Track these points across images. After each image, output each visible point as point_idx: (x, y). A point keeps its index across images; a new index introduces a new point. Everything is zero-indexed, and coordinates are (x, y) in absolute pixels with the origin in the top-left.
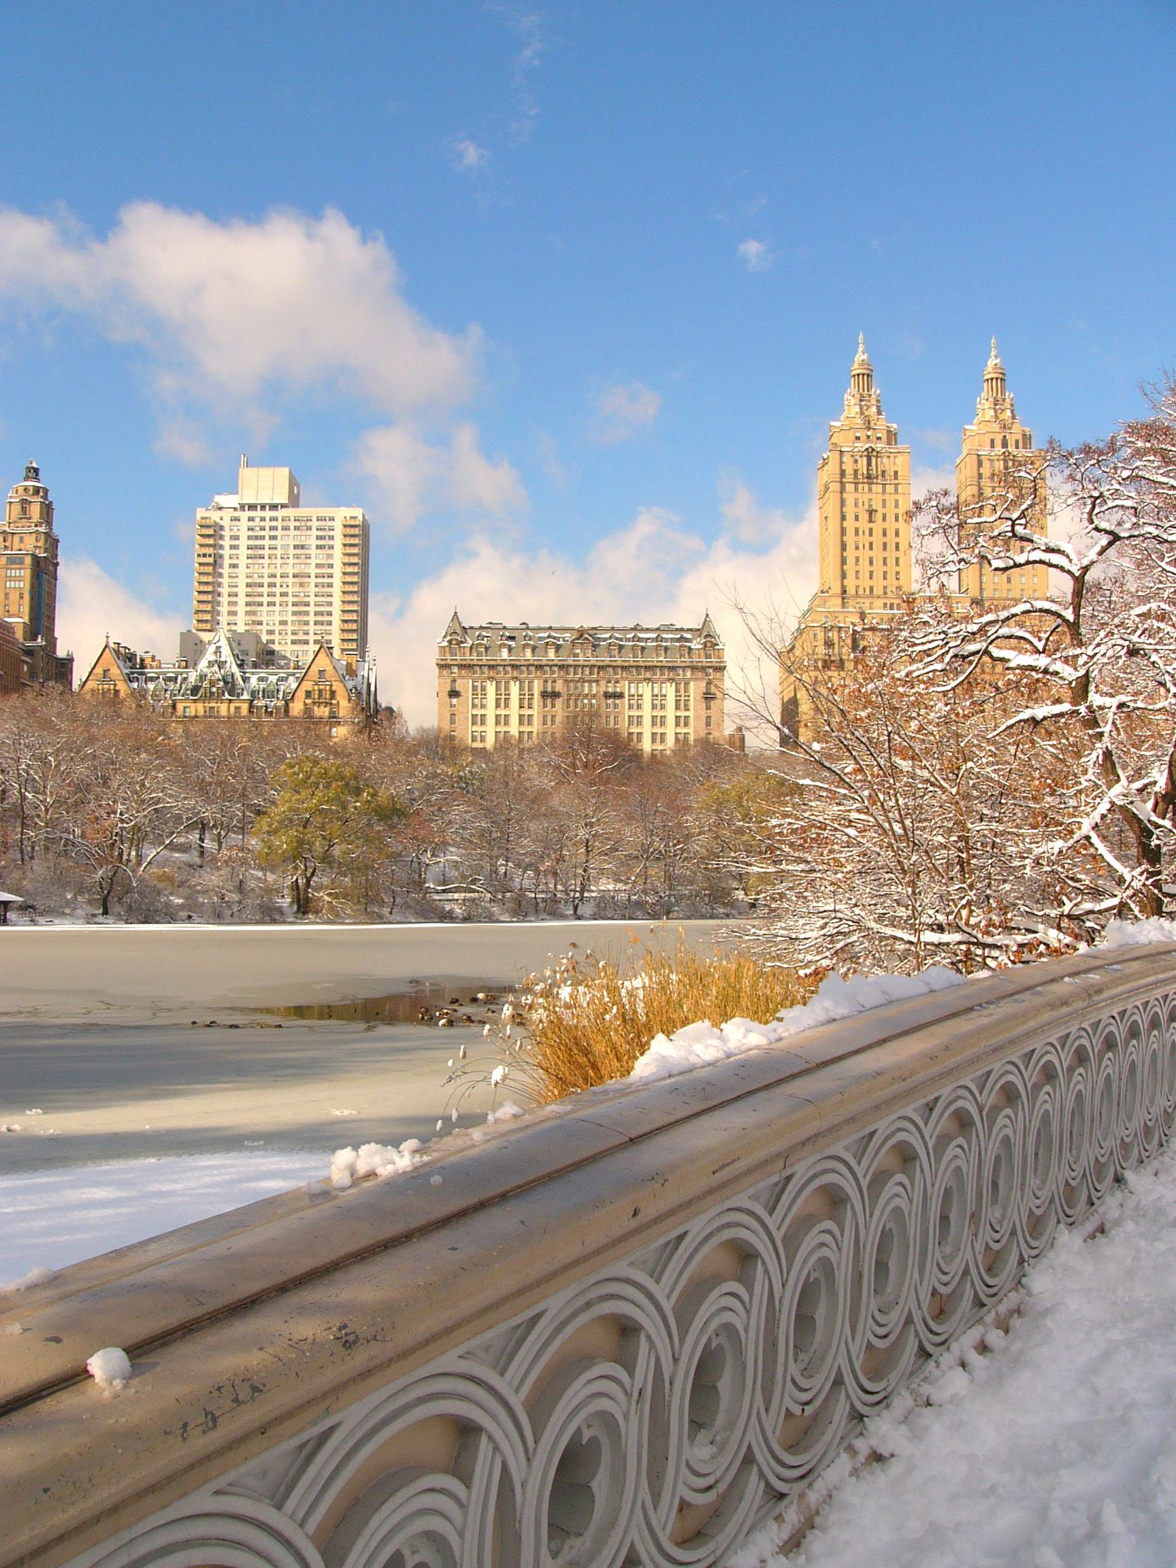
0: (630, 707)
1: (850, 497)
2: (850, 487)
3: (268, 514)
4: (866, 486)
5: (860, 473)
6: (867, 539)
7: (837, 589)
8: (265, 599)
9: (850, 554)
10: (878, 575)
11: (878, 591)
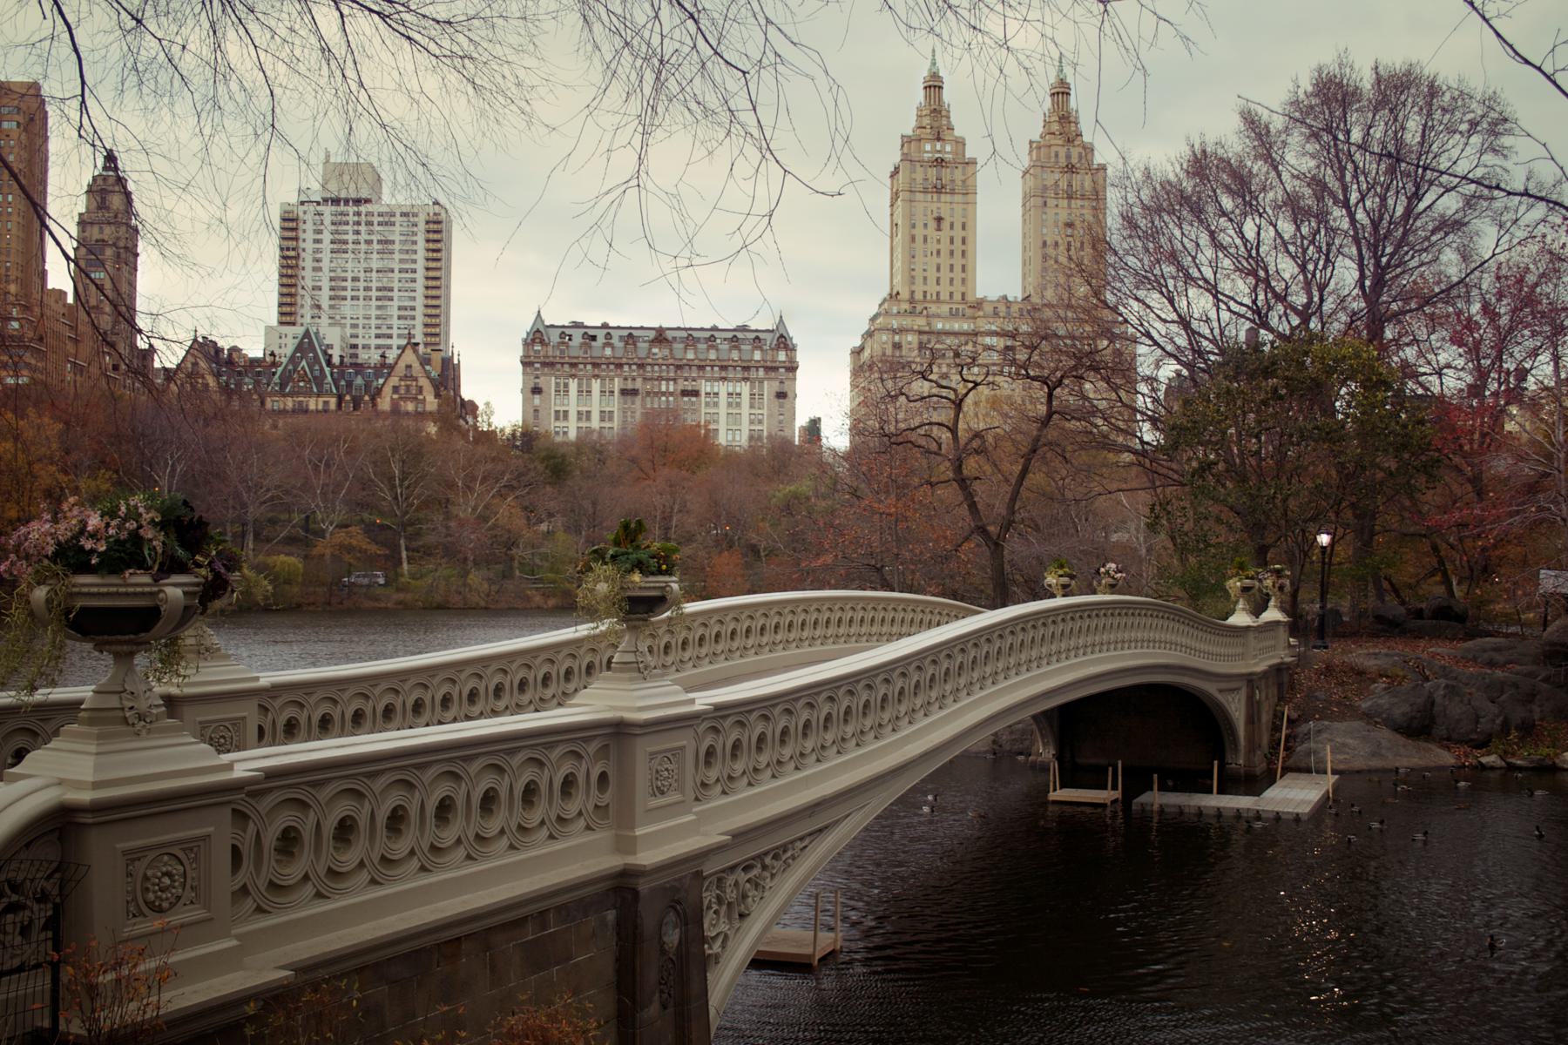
0: (707, 404)
3: (351, 209)
8: (349, 294)
10: (945, 281)
11: (945, 296)
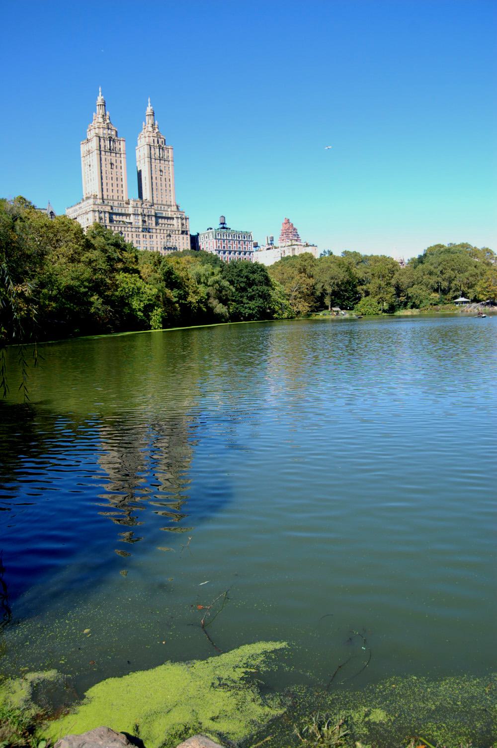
1: (103, 157)
2: (103, 153)
4: (109, 153)
5: (106, 147)
6: (110, 176)
7: (99, 196)
9: (104, 181)
10: (115, 191)
11: (115, 198)
